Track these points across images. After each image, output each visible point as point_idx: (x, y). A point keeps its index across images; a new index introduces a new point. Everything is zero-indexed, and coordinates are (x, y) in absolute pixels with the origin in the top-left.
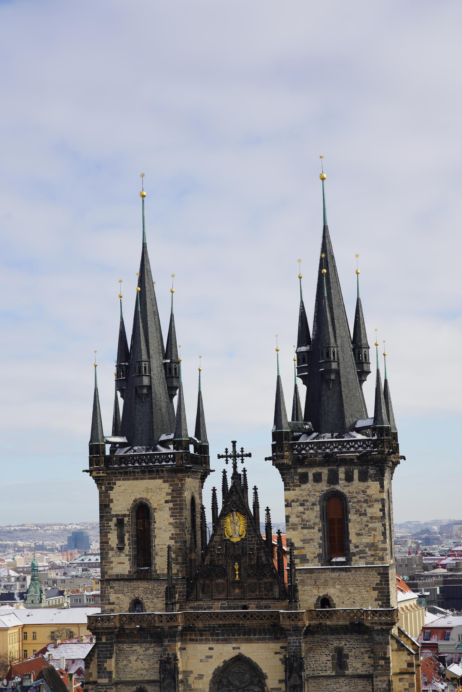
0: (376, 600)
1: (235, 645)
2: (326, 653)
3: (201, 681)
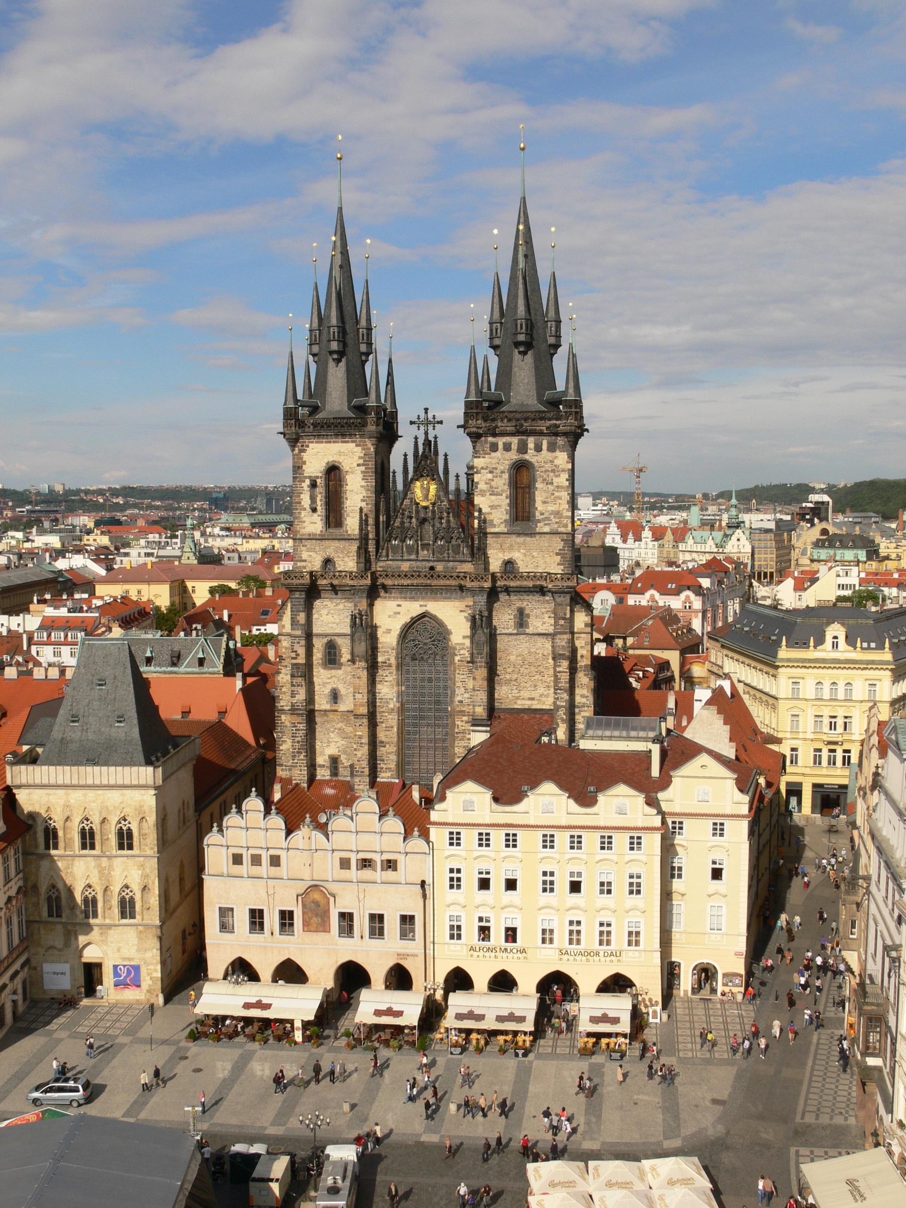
0: (558, 564)
1: (422, 603)
2: (510, 612)
3: (389, 635)
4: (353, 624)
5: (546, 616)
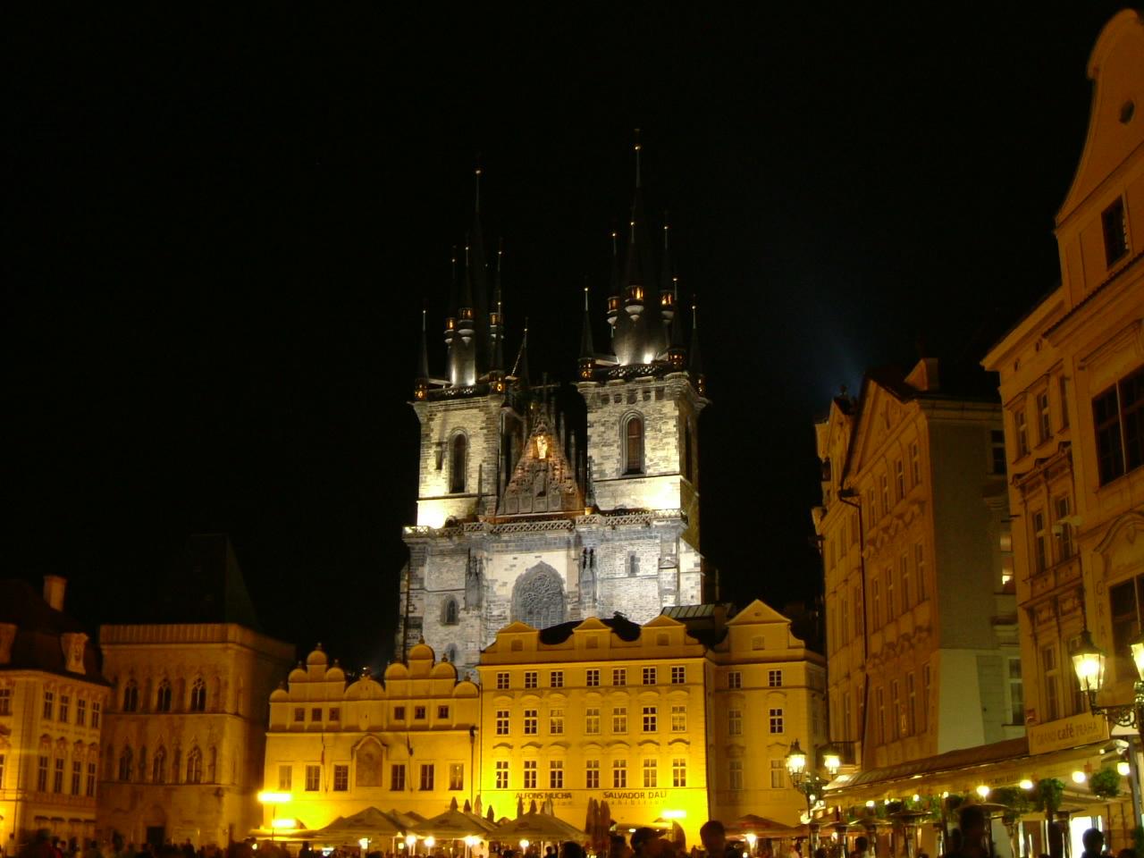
1: (537, 554)
3: (505, 588)
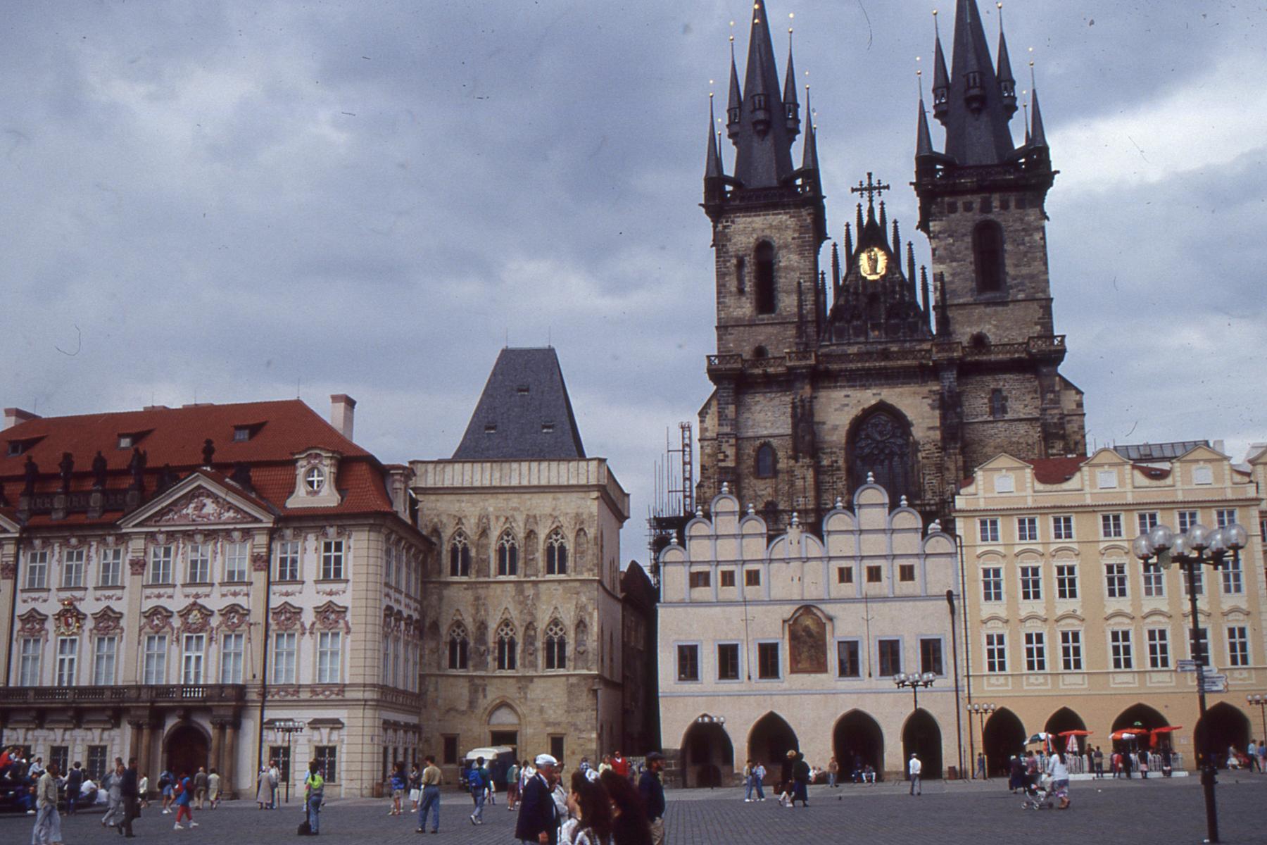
4: (794, 416)
5: (1028, 398)
